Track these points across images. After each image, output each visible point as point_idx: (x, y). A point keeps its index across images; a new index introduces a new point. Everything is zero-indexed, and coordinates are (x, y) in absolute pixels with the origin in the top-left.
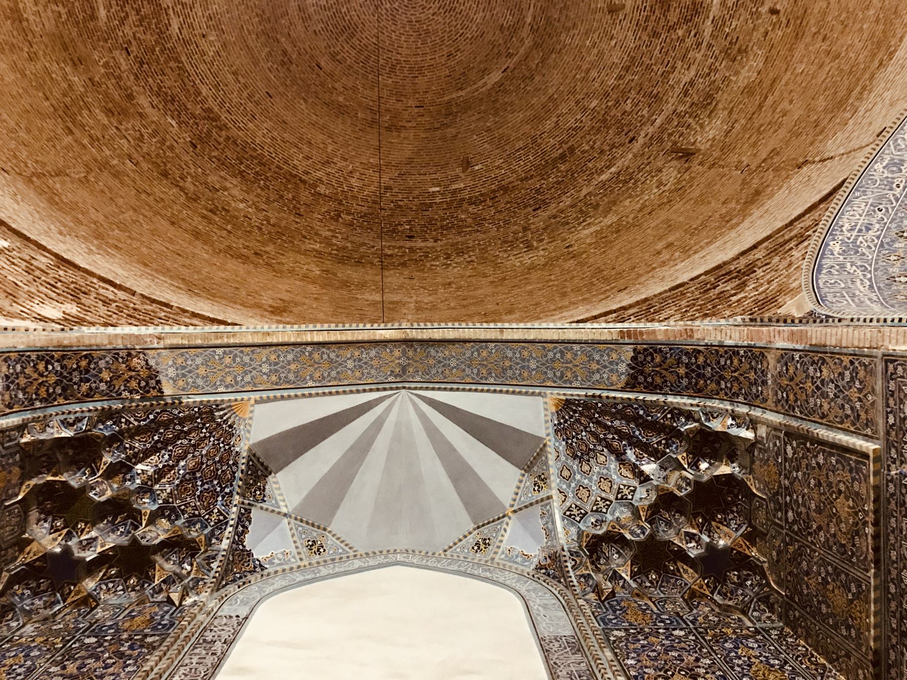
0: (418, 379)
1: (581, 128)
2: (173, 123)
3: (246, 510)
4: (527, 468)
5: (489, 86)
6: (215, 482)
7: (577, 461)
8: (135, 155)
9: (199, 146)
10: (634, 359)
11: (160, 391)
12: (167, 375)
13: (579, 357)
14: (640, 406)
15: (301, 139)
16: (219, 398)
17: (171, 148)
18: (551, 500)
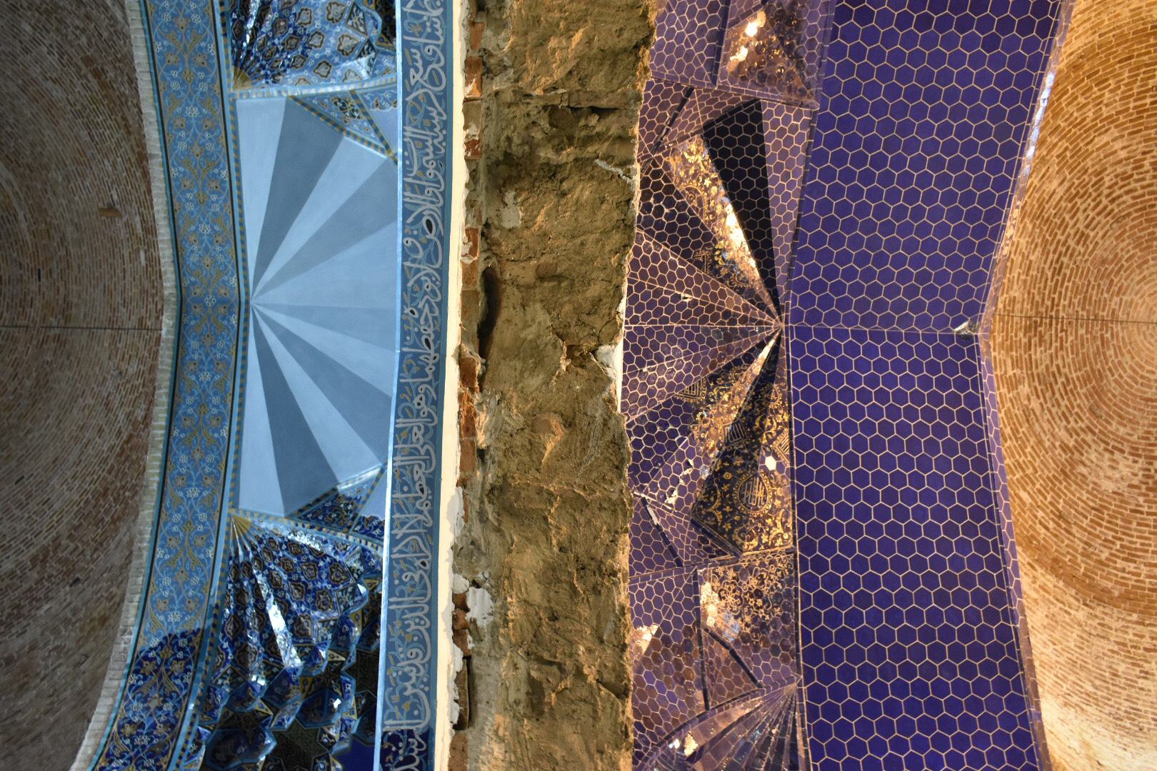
0: (234, 280)
1: (60, 47)
2: (46, 607)
4: (339, 128)
5: (11, 176)
7: (310, 53)
8: (77, 657)
9: (78, 575)
11: (194, 633)
12: (177, 623)
15: (76, 439)
16: (220, 556)
17: (75, 612)
18: (358, 93)
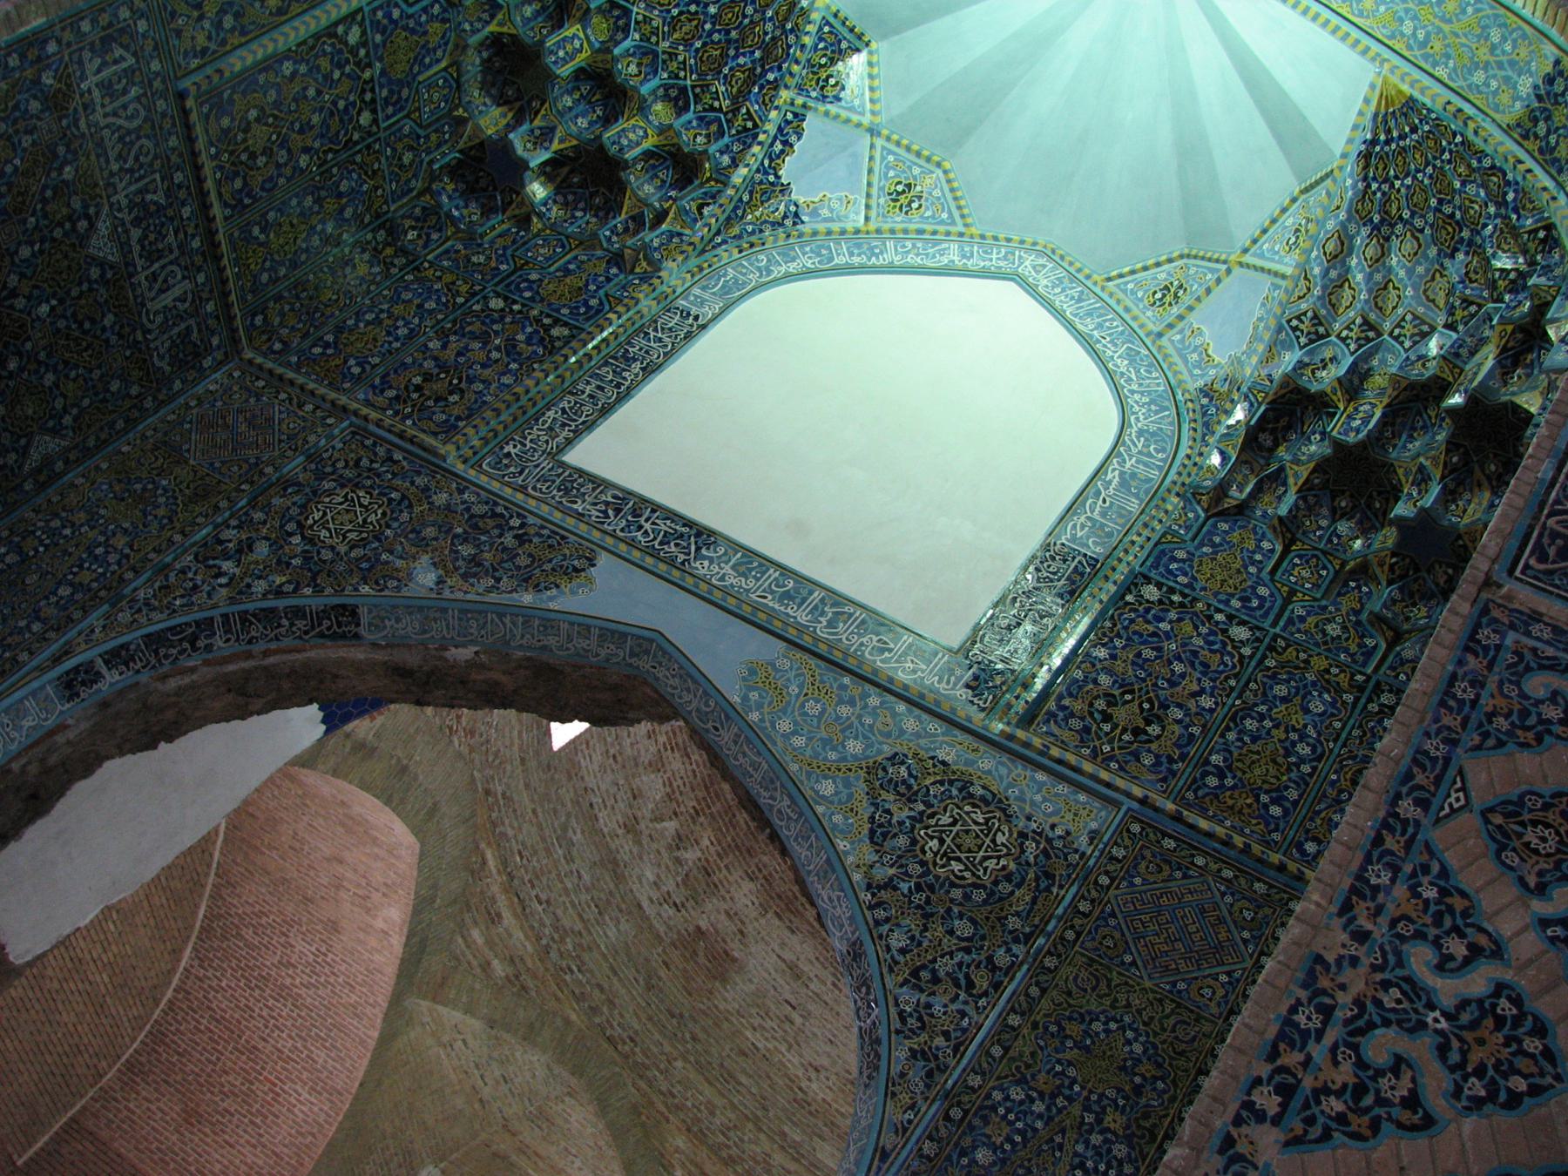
3: (796, 115)
6: (758, 54)
10: (1550, 80)
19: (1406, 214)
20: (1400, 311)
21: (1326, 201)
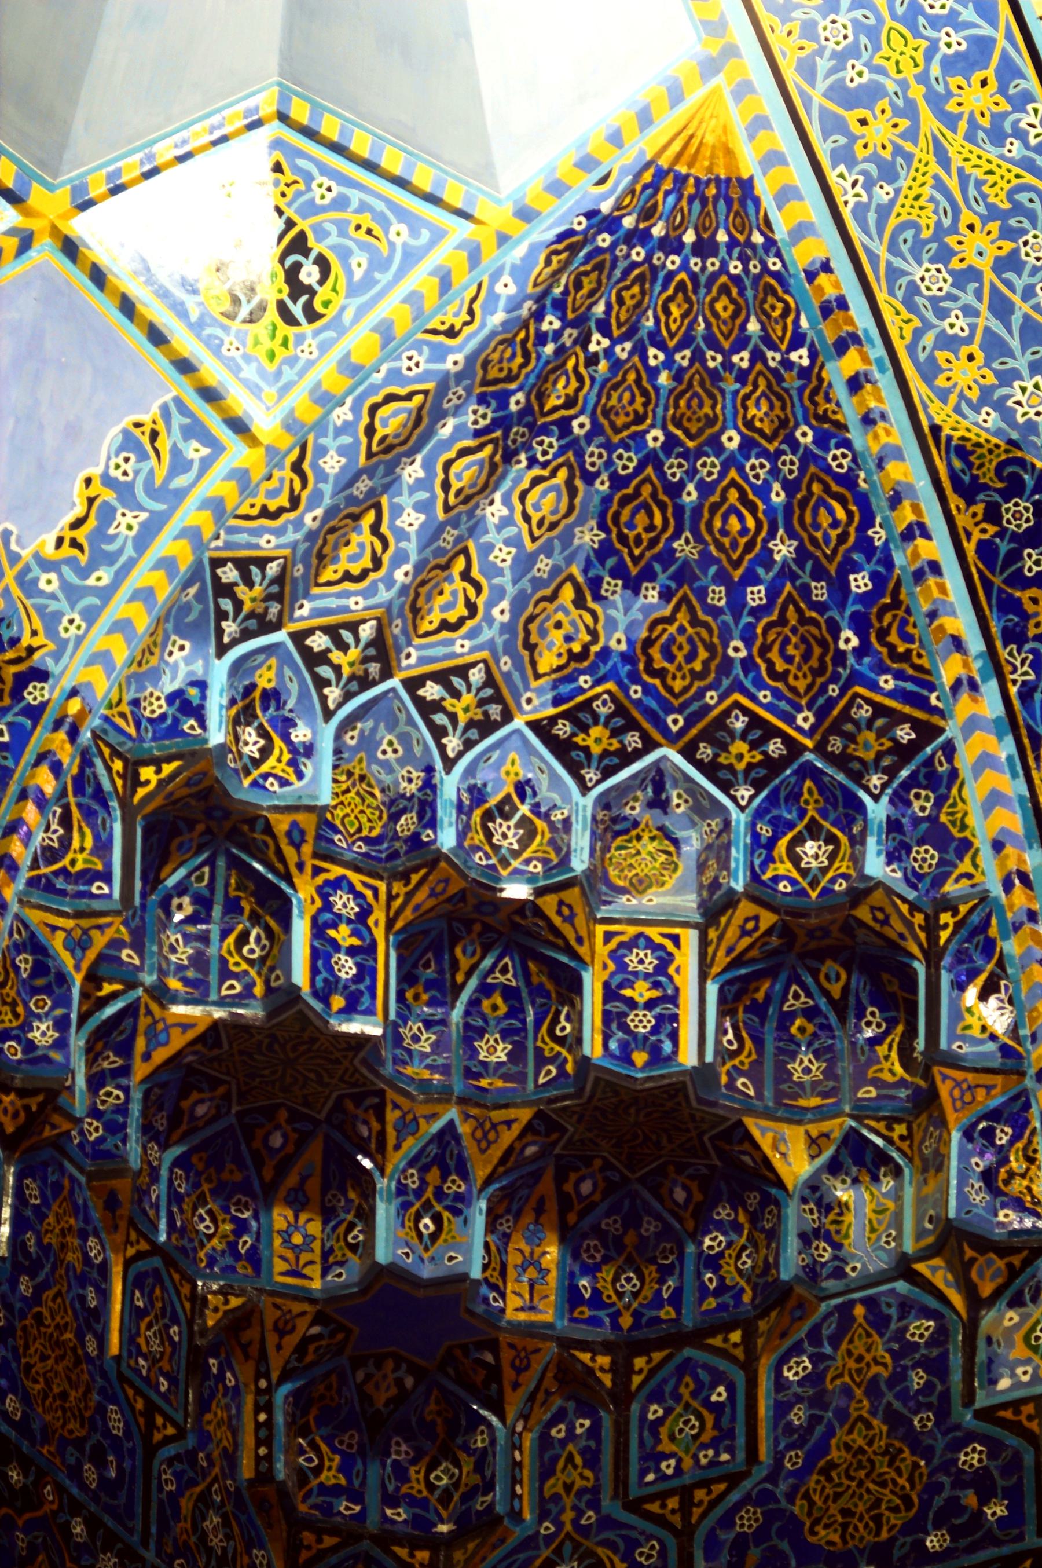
13: (991, 152)
14: (888, 562)
19: (581, 424)
20: (461, 646)
21: (431, 299)
